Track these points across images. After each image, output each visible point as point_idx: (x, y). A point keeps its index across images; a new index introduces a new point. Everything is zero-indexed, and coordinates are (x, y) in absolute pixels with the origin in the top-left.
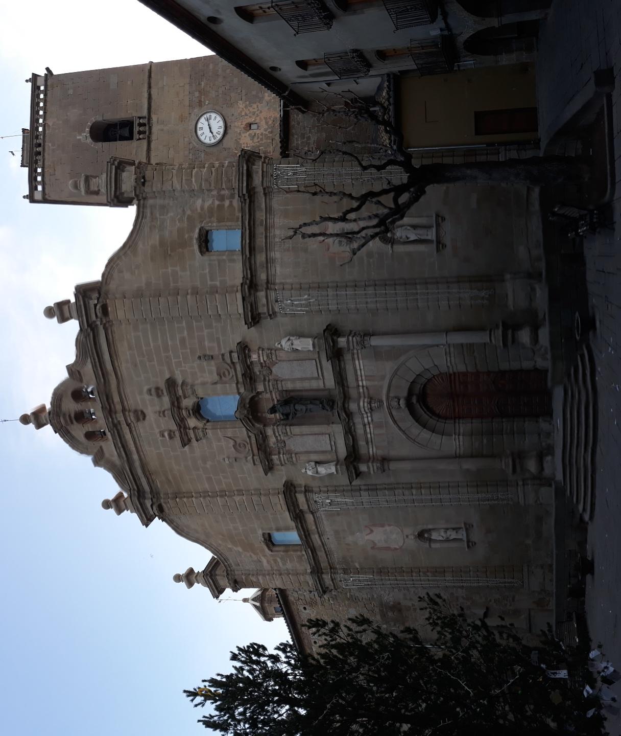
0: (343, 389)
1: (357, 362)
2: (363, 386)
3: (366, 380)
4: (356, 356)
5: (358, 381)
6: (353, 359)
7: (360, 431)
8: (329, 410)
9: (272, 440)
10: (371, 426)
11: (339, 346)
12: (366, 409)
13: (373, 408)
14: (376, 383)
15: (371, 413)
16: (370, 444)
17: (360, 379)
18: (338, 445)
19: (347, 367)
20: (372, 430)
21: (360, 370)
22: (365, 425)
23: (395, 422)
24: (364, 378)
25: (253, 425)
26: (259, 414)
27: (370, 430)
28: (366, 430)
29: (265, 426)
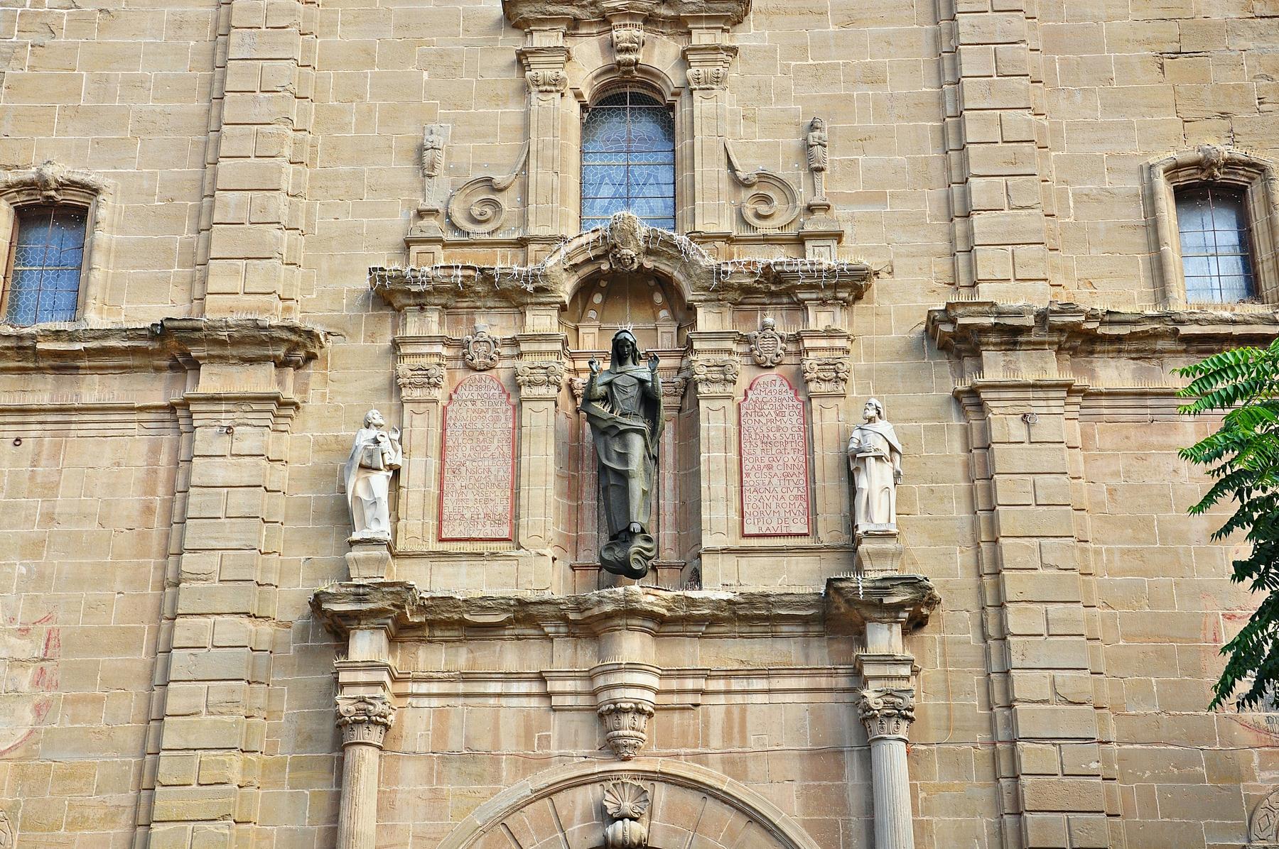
0: (700, 620)
1: (803, 683)
2: (703, 692)
3: (729, 705)
4: (823, 682)
5: (726, 677)
6: (814, 672)
7: (508, 655)
8: (606, 556)
9: (494, 326)
10: (534, 702)
11: (870, 627)
12: (617, 694)
13: (611, 721)
14: (716, 742)
15: (593, 709)
16: (461, 688)
17: (736, 685)
18: (464, 567)
19: (781, 645)
20: (514, 702)
21: (769, 691)
22: (541, 678)
23: (549, 793)
24: (738, 699)
25: (575, 267)
26: (598, 299)
27: (518, 695)
28: (519, 680)
29: (563, 308)
